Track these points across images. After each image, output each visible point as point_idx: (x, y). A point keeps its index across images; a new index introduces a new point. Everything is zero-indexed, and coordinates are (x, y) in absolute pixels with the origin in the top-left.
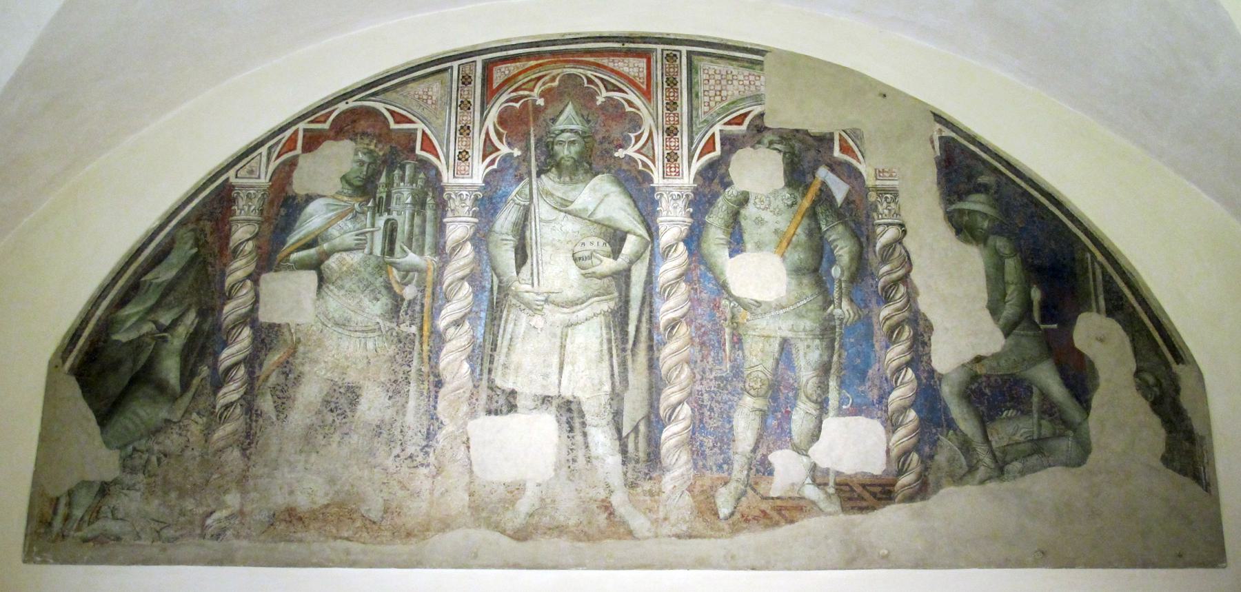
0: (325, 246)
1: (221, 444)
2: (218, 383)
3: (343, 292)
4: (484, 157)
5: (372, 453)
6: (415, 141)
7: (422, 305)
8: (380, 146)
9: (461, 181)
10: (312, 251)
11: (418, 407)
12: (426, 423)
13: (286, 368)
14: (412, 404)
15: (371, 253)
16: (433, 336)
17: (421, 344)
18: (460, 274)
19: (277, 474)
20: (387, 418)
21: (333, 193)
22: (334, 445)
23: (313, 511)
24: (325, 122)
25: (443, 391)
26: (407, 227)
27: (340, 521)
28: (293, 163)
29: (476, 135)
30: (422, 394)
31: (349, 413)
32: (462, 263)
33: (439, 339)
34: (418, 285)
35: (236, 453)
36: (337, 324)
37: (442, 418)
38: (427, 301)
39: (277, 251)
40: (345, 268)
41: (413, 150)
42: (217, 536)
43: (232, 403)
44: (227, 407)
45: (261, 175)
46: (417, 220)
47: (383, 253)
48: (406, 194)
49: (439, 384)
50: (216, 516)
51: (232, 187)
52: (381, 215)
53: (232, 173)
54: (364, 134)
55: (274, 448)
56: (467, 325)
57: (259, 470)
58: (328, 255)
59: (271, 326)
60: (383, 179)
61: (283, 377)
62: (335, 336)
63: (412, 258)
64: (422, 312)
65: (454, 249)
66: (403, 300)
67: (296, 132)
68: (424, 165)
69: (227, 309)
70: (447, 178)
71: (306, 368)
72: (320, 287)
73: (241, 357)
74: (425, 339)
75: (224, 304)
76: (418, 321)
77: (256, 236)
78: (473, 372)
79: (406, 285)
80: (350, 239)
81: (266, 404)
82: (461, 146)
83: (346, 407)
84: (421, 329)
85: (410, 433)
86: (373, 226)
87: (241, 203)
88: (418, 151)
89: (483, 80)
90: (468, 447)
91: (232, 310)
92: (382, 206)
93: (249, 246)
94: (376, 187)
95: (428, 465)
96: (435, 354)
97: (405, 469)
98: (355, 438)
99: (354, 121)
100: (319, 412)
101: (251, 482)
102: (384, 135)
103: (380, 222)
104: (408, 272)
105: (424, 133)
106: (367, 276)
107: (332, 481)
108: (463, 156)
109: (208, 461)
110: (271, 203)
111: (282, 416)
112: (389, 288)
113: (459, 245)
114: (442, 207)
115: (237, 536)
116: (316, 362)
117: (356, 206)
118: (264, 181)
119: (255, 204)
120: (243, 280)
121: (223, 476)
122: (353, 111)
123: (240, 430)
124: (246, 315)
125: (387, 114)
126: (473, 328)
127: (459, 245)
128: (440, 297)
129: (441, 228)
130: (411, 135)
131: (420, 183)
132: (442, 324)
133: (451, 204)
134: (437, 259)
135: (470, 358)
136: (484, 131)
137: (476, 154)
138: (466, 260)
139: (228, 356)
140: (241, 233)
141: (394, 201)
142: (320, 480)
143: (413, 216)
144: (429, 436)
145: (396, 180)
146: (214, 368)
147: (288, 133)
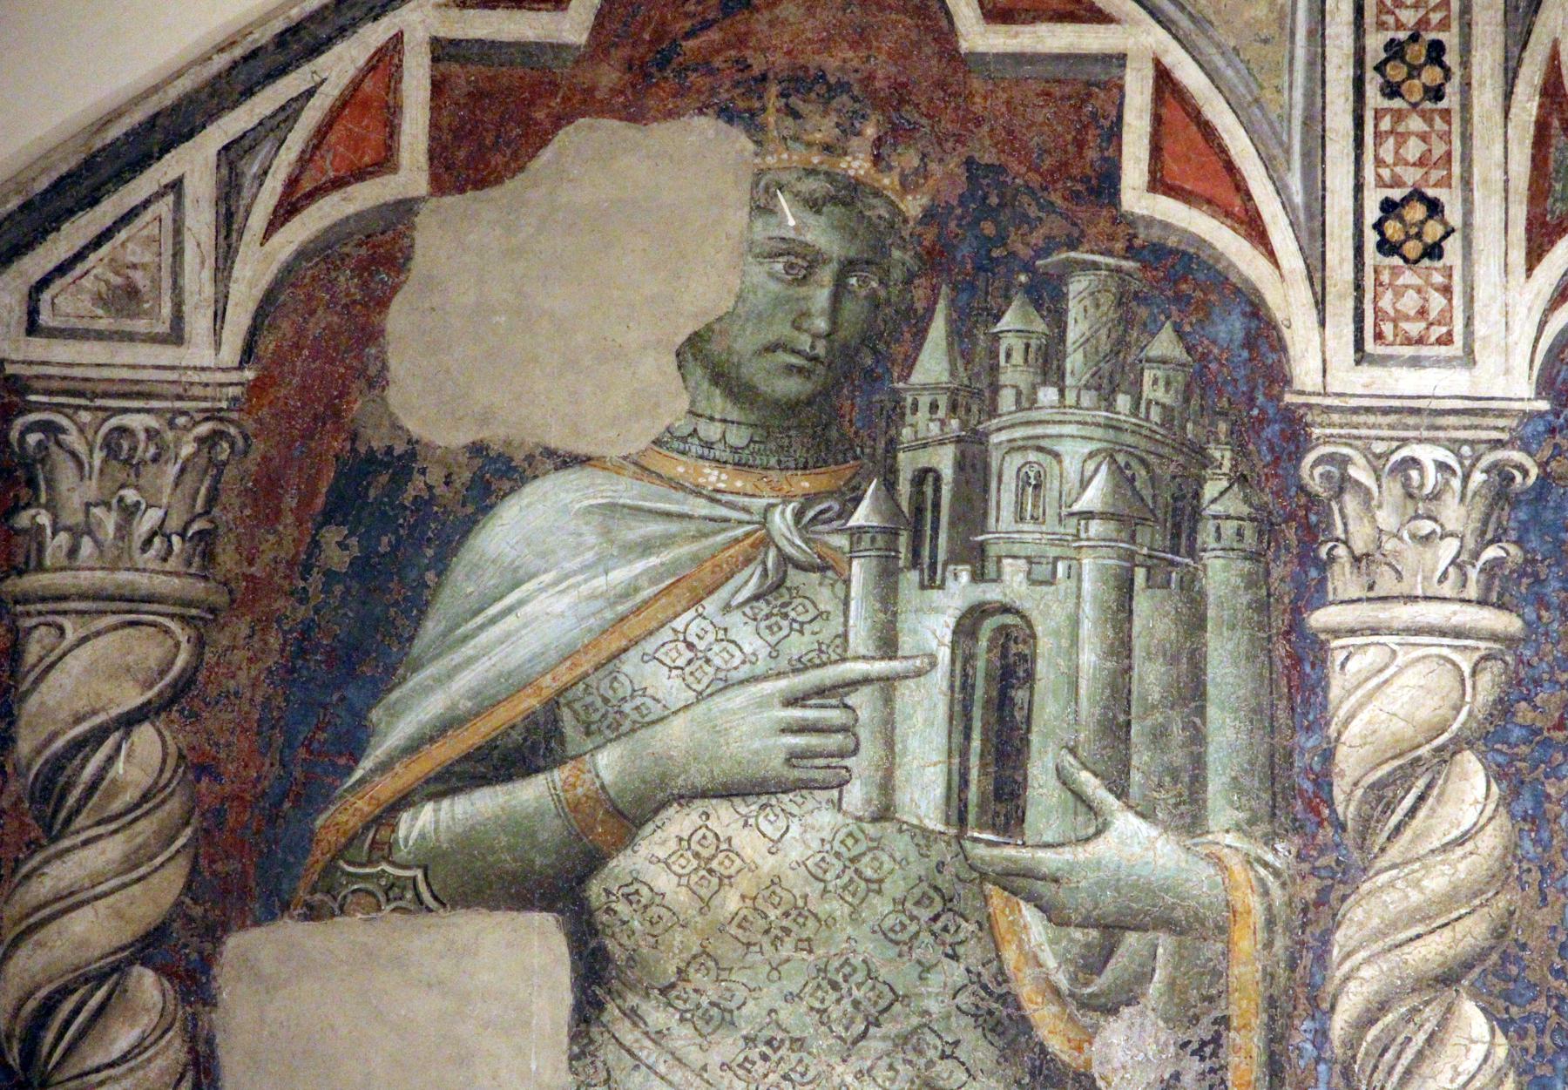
0: (609, 763)
3: (727, 1047)
6: (1114, 133)
8: (909, 159)
9: (1405, 382)
10: (529, 793)
15: (884, 813)
18: (1431, 950)
21: (638, 440)
26: (1089, 658)
28: (380, 251)
29: (1486, 98)
32: (1436, 882)
34: (1181, 1013)
39: (310, 793)
40: (731, 902)
41: (1106, 183)
46: (1152, 615)
47: (958, 814)
48: (1074, 453)
52: (931, 582)
54: (803, 84)
58: (628, 816)
60: (933, 364)
63: (1134, 845)
65: (1381, 795)
67: (387, 59)
68: (1174, 280)
70: (1317, 359)
72: (587, 1012)
77: (176, 699)
79: (1109, 1008)
80: (751, 728)
82: (1402, 159)
86: (888, 645)
87: (74, 490)
88: (1136, 196)
92: (936, 528)
93: (141, 758)
94: (896, 412)
103: (931, 624)
104: (1112, 929)
105: (1164, 79)
106: (868, 948)
108: (1411, 229)
114: (1295, 536)
117: (781, 522)
118: (210, 354)
119: (163, 499)
120: (113, 971)
127: (1412, 773)
129: (1296, 673)
130: (1093, 83)
131: (1154, 390)
133: (1355, 525)
134: (1282, 854)
137: (1488, 215)
138: (1466, 867)
140: (85, 677)
141: (1005, 497)
143: (1125, 588)
145: (1014, 374)
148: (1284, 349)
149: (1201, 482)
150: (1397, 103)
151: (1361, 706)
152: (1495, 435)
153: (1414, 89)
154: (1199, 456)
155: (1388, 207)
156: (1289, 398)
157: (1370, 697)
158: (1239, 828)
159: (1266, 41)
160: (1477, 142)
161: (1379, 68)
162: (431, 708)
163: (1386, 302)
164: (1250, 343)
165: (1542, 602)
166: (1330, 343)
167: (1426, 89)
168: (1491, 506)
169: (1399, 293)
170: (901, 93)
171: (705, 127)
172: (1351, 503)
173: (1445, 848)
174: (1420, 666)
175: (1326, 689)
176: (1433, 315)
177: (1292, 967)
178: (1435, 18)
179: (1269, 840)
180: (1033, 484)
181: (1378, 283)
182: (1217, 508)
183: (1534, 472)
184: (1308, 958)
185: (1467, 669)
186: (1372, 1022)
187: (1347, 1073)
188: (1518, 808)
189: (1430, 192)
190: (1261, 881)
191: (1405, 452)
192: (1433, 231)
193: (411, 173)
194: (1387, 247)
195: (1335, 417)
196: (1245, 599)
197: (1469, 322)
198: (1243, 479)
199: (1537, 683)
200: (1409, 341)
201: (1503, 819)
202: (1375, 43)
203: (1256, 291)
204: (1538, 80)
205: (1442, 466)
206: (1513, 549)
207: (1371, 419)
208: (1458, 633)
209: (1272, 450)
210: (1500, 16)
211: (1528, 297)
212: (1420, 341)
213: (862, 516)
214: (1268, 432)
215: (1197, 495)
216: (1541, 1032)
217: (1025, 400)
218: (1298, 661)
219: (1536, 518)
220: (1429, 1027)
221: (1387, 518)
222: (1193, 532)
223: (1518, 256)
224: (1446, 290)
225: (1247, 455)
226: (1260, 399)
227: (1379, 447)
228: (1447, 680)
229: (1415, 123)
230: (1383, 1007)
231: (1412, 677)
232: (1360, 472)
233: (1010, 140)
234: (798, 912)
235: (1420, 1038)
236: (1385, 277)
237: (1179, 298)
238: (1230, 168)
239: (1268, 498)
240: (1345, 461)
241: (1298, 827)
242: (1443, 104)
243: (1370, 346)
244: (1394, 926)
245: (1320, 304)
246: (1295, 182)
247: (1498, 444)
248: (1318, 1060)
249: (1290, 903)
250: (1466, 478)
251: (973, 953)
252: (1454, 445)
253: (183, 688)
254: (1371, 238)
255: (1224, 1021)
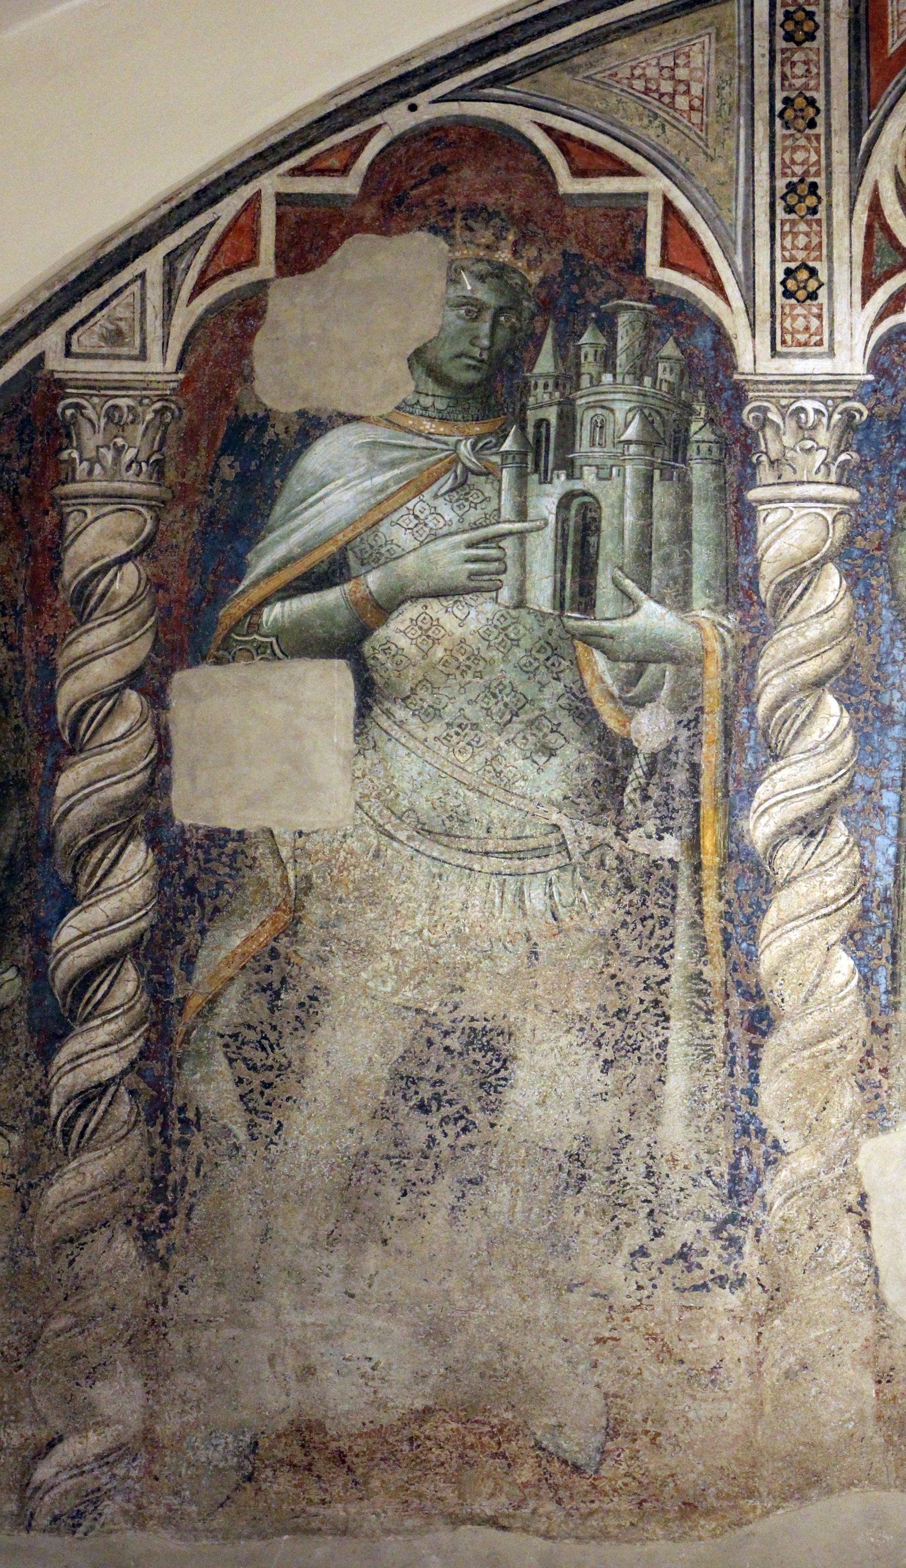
0: (373, 580)
1: (75, 1218)
2: (53, 1019)
3: (437, 729)
4: (869, 289)
5: (558, 1242)
6: (642, 236)
7: (695, 770)
8: (532, 252)
10: (332, 596)
11: (696, 1095)
12: (725, 1147)
13: (269, 971)
14: (677, 1084)
15: (520, 604)
16: (734, 871)
17: (698, 895)
18: (810, 669)
19: (261, 1312)
20: (601, 1131)
21: (387, 407)
22: (439, 1218)
23: (379, 1433)
24: (344, 171)
25: (773, 1045)
27: (466, 1462)
28: (249, 309)
29: (840, 213)
30: (708, 1055)
31: (479, 1117)
32: (813, 633)
33: (753, 879)
34: (678, 706)
35: (125, 1246)
36: (424, 830)
37: (776, 1130)
38: (709, 756)
39: (216, 598)
40: (439, 653)
41: (638, 262)
42: (72, 1521)
43: (102, 1087)
44: (86, 1098)
45: (143, 350)
46: (663, 496)
47: (560, 603)
48: (621, 409)
49: (761, 1022)
50: (69, 1450)
51: (57, 387)
52: (545, 480)
53: (51, 339)
54: (474, 212)
55: (246, 1228)
56: (839, 834)
57: (202, 1301)
58: (384, 608)
59: (217, 837)
60: (545, 363)
61: (260, 1001)
62: (421, 869)
63: (654, 618)
64: (695, 790)
65: (784, 588)
66: (631, 752)
67: (252, 205)
68: (676, 313)
69: (68, 782)
70: (751, 355)
71: (337, 970)
72: (363, 711)
73: (123, 937)
74: (709, 877)
75: (57, 769)
76: (682, 819)
77: (145, 549)
78: (867, 982)
79: (639, 703)
80: (449, 559)
81: (213, 1087)
82: (795, 248)
83: (468, 1096)
84: (694, 845)
85: (678, 1179)
86: (522, 514)
87: (91, 440)
88: (654, 269)
89: (854, 24)
90: (866, 1225)
91: (84, 787)
92: (548, 450)
94: (526, 389)
95: (741, 1282)
96: (742, 926)
97: (665, 1295)
98: (501, 1196)
99: (439, 170)
100: (383, 1113)
101: (177, 1341)
102: (538, 215)
103: (545, 503)
104: (642, 662)
105: (669, 207)
107: (435, 1334)
108: (801, 284)
109: (33, 1273)
110: (190, 437)
111: (266, 1127)
112: (584, 712)
113: (801, 575)
114: (739, 451)
115: (139, 1519)
116: (362, 951)
117: (465, 449)
118: (160, 366)
119: (137, 443)
120: (115, 692)
121: (83, 1322)
122: (433, 134)
123: (132, 1171)
124: (130, 806)
125: (545, 145)
126: (861, 841)
127: (801, 575)
128: (751, 745)
129: (740, 524)
130: (630, 211)
131: (665, 373)
132: (759, 830)
134: (732, 621)
135: (853, 939)
136: (864, 199)
137: (841, 276)
138: (828, 624)
139: (83, 934)
140: (97, 539)
141: (584, 434)
142: (399, 1331)
143: (649, 480)
144: (739, 1187)
145: (589, 367)
146: (38, 972)
147: (229, 207)
148: (733, 350)
149: (689, 423)
150: (793, 216)
151: (774, 541)
152: (845, 394)
153: (802, 208)
154: (688, 408)
155: (789, 272)
156: (736, 377)
157: (779, 536)
158: (709, 608)
159: (723, 184)
160: (835, 236)
161: (783, 198)
162: (280, 551)
163: (787, 324)
164: (715, 348)
165: (870, 483)
166: (758, 347)
167: (808, 208)
168: (843, 432)
169: (794, 318)
170: (527, 216)
171: (423, 236)
172: (769, 432)
173: (818, 615)
174: (806, 519)
175: (756, 532)
176: (813, 330)
177: (737, 680)
178: (813, 170)
179: (725, 614)
180: (599, 426)
181: (783, 314)
182: (698, 437)
183: (866, 413)
184: (745, 675)
185: (830, 519)
186: (779, 707)
187: (765, 735)
188: (856, 593)
189: (811, 264)
190: (721, 635)
191: (798, 404)
192: (812, 285)
193: (266, 267)
194: (787, 294)
195: (761, 386)
196: (713, 485)
197: (831, 333)
198: (711, 421)
199: (867, 526)
200: (799, 344)
201: (848, 599)
202: (781, 184)
203: (718, 319)
204: (867, 202)
205: (817, 411)
206: (855, 455)
207: (780, 387)
208: (826, 501)
209: (727, 405)
210: (847, 168)
211: (862, 319)
212: (806, 344)
213: (508, 445)
214: (726, 395)
215: (687, 430)
216: (866, 710)
217: (596, 381)
218: (740, 517)
219: (867, 438)
220: (808, 709)
221: (788, 440)
222: (685, 449)
223: (857, 297)
224: (819, 317)
225: (714, 408)
226: (721, 377)
227: (784, 402)
228: (819, 526)
229: (803, 227)
230: (784, 700)
231: (800, 525)
232: (774, 416)
233: (586, 240)
234: (475, 657)
235: (803, 716)
236: (787, 310)
237: (677, 324)
238: (704, 253)
239: (724, 431)
240: (765, 410)
241: (740, 606)
242: (817, 217)
243: (779, 347)
244: (790, 657)
245: (753, 325)
246: (739, 260)
247: (847, 399)
248: (750, 728)
249: (736, 646)
250: (830, 417)
251: (568, 677)
252: (824, 400)
253: (149, 542)
254: (779, 289)
255: (701, 709)
